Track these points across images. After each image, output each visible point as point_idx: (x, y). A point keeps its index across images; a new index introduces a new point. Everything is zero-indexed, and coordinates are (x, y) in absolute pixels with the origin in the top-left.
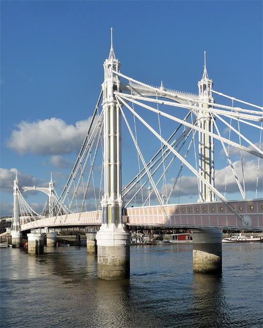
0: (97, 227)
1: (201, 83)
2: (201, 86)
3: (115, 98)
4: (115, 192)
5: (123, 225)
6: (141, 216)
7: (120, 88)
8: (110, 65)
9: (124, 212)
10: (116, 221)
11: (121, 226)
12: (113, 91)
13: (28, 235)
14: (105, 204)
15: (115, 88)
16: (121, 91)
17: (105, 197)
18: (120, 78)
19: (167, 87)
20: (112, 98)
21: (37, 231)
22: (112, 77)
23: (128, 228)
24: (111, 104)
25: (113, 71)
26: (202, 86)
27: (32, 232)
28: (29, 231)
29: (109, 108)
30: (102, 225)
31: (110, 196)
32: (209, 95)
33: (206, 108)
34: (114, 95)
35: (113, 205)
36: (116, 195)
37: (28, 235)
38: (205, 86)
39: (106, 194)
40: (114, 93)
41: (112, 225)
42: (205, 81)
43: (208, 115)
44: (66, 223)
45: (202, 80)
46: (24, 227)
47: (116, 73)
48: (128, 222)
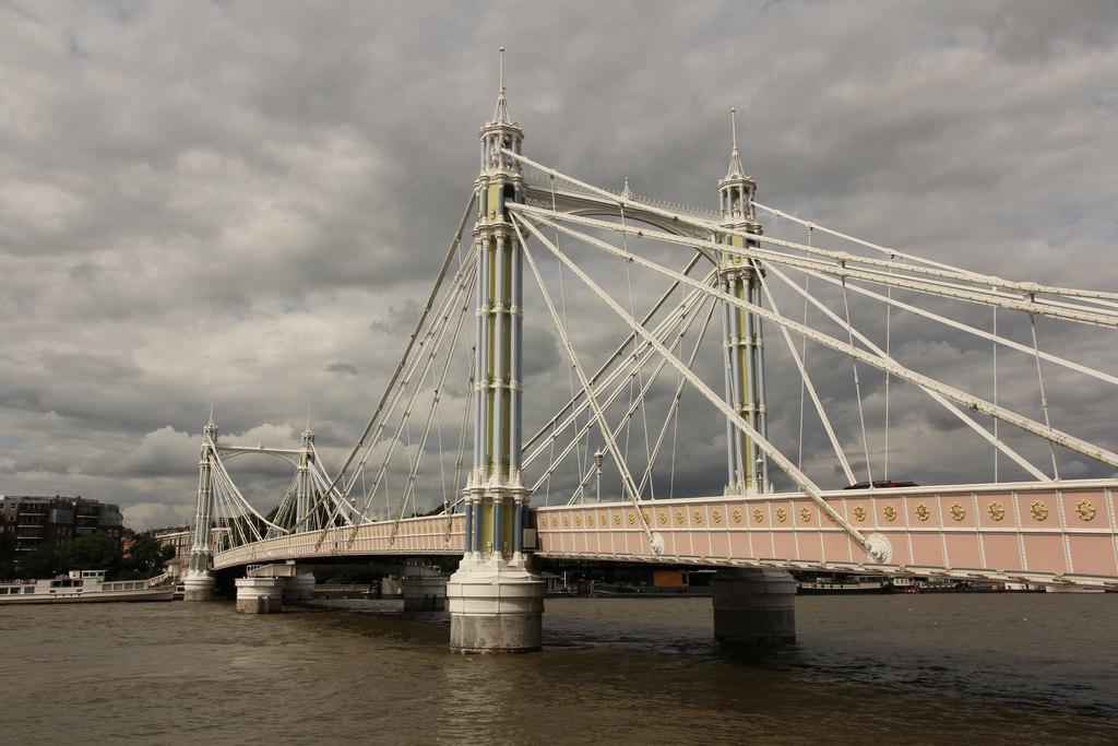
0: (450, 563)
3: (507, 219)
4: (505, 463)
5: (525, 557)
9: (529, 518)
11: (518, 558)
13: (238, 582)
14: (475, 497)
15: (508, 192)
17: (476, 477)
20: (500, 220)
21: (268, 571)
23: (537, 564)
24: (498, 233)
27: (249, 573)
28: (240, 571)
29: (493, 241)
30: (466, 554)
33: (738, 249)
36: (505, 472)
37: (238, 582)
39: (479, 470)
40: (507, 204)
43: (745, 264)
45: (728, 179)
46: (223, 560)
47: (511, 153)
48: (538, 546)
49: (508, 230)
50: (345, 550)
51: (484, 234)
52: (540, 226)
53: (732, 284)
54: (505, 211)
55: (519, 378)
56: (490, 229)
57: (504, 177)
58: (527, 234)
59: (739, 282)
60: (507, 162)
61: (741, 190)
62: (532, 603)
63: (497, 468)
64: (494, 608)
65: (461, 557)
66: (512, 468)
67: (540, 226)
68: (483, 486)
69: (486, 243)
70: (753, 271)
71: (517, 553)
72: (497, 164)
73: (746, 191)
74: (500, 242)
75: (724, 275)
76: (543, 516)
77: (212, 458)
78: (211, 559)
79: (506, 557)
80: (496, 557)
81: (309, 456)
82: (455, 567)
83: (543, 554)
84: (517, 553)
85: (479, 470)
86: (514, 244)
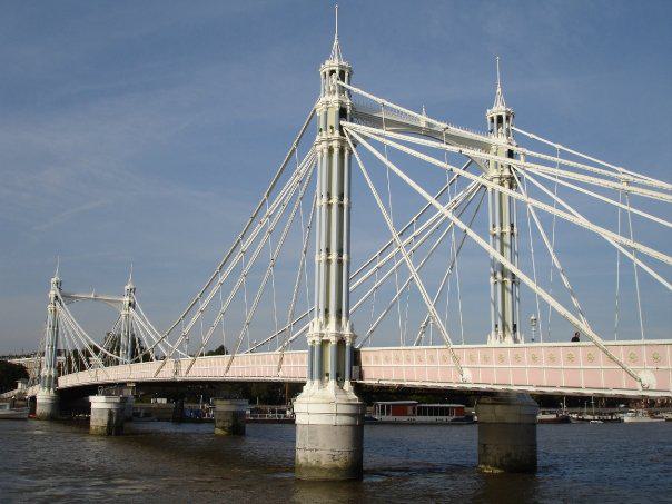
0: (296, 388)
3: (342, 134)
6: (385, 366)
8: (333, 72)
9: (356, 357)
11: (347, 385)
14: (317, 340)
15: (342, 114)
16: (352, 121)
20: (337, 134)
22: (337, 94)
23: (359, 389)
24: (335, 144)
26: (495, 118)
28: (93, 389)
29: (331, 150)
30: (309, 382)
31: (327, 322)
32: (508, 135)
34: (341, 127)
35: (333, 340)
37: (92, 399)
38: (500, 118)
39: (317, 320)
40: (342, 123)
45: (495, 109)
46: (66, 381)
47: (345, 85)
48: (361, 378)
49: (343, 142)
50: (182, 377)
51: (324, 144)
52: (365, 138)
55: (348, 253)
56: (329, 140)
57: (341, 103)
58: (356, 144)
60: (342, 90)
61: (504, 118)
62: (360, 423)
63: (333, 319)
64: (334, 420)
65: (304, 384)
66: (344, 318)
67: (365, 138)
68: (323, 331)
69: (325, 151)
70: (513, 178)
72: (334, 92)
73: (508, 119)
74: (336, 151)
76: (367, 354)
77: (57, 303)
78: (56, 382)
80: (332, 383)
81: (130, 304)
82: (301, 391)
85: (317, 320)
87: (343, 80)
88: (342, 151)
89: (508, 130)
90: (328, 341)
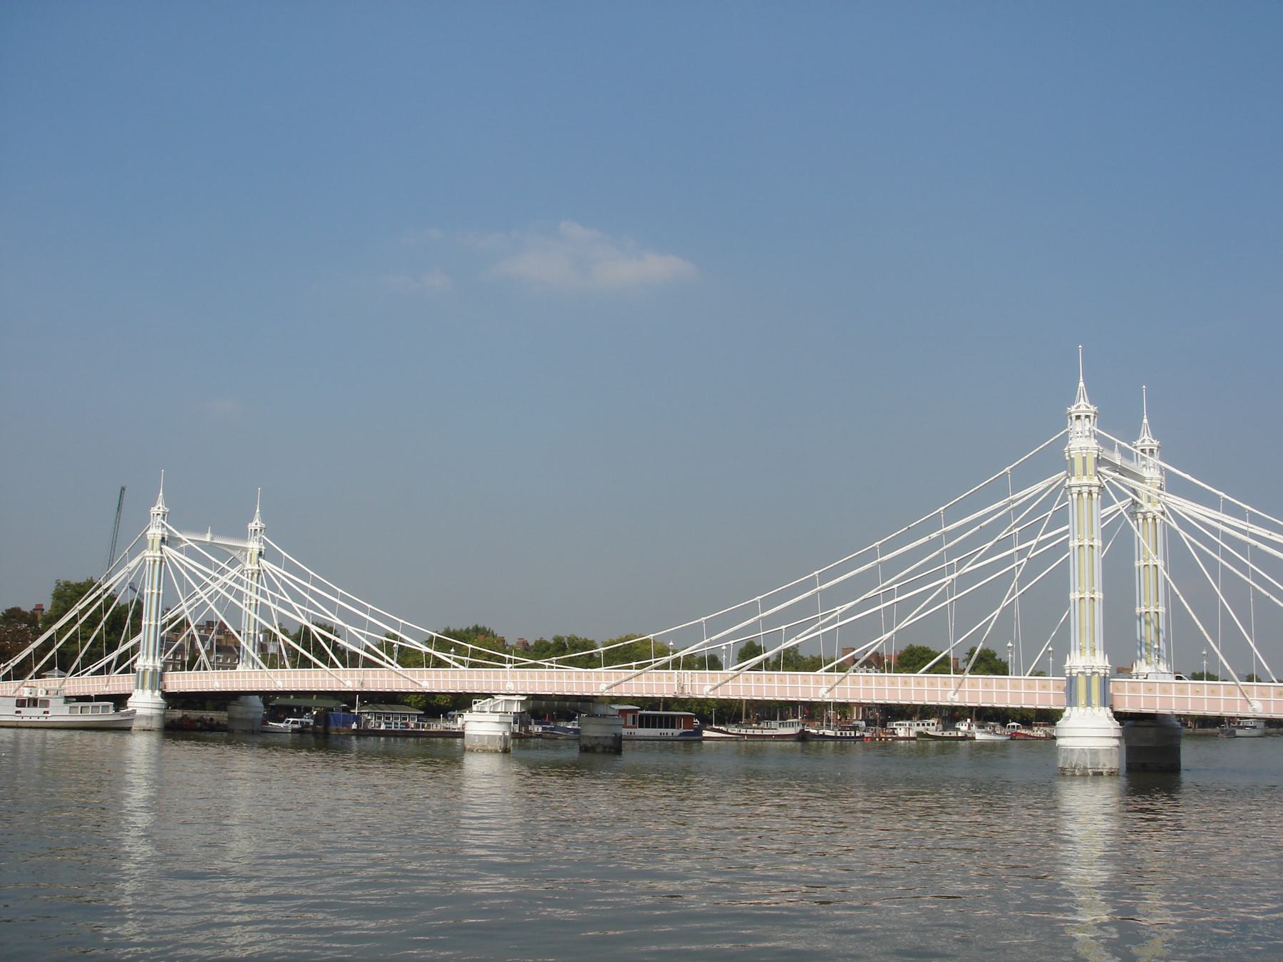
1: (252, 526)
2: (251, 530)
4: (154, 655)
7: (167, 542)
8: (158, 514)
10: (153, 688)
11: (157, 693)
12: (161, 544)
15: (163, 540)
18: (168, 530)
19: (216, 533)
22: (160, 528)
24: (158, 559)
25: (162, 521)
29: (155, 561)
32: (260, 542)
34: (161, 549)
35: (151, 669)
40: (162, 546)
41: (149, 692)
42: (256, 524)
44: (107, 689)
47: (165, 523)
48: (165, 688)
49: (162, 557)
53: (250, 575)
54: (161, 549)
59: (253, 574)
63: (151, 657)
66: (157, 657)
71: (157, 691)
72: (159, 526)
73: (261, 530)
74: (158, 563)
75: (247, 570)
79: (153, 692)
83: (167, 691)
84: (157, 691)
86: (163, 564)
87: (164, 520)
88: (161, 562)
89: (260, 538)
90: (148, 669)
